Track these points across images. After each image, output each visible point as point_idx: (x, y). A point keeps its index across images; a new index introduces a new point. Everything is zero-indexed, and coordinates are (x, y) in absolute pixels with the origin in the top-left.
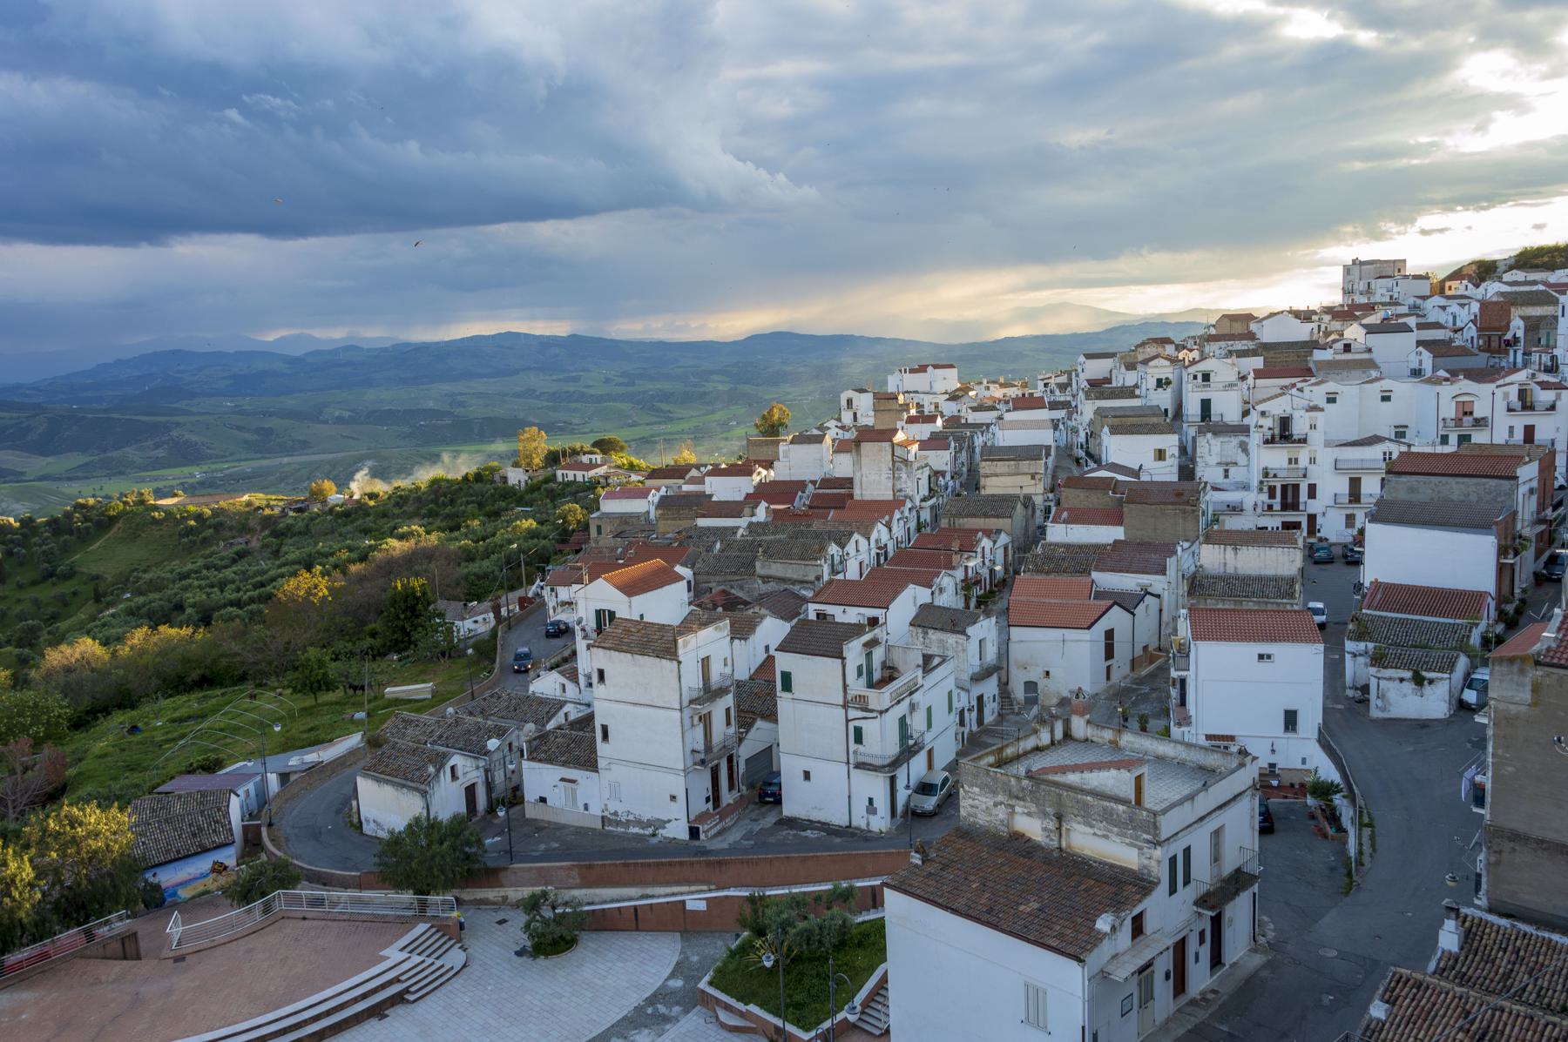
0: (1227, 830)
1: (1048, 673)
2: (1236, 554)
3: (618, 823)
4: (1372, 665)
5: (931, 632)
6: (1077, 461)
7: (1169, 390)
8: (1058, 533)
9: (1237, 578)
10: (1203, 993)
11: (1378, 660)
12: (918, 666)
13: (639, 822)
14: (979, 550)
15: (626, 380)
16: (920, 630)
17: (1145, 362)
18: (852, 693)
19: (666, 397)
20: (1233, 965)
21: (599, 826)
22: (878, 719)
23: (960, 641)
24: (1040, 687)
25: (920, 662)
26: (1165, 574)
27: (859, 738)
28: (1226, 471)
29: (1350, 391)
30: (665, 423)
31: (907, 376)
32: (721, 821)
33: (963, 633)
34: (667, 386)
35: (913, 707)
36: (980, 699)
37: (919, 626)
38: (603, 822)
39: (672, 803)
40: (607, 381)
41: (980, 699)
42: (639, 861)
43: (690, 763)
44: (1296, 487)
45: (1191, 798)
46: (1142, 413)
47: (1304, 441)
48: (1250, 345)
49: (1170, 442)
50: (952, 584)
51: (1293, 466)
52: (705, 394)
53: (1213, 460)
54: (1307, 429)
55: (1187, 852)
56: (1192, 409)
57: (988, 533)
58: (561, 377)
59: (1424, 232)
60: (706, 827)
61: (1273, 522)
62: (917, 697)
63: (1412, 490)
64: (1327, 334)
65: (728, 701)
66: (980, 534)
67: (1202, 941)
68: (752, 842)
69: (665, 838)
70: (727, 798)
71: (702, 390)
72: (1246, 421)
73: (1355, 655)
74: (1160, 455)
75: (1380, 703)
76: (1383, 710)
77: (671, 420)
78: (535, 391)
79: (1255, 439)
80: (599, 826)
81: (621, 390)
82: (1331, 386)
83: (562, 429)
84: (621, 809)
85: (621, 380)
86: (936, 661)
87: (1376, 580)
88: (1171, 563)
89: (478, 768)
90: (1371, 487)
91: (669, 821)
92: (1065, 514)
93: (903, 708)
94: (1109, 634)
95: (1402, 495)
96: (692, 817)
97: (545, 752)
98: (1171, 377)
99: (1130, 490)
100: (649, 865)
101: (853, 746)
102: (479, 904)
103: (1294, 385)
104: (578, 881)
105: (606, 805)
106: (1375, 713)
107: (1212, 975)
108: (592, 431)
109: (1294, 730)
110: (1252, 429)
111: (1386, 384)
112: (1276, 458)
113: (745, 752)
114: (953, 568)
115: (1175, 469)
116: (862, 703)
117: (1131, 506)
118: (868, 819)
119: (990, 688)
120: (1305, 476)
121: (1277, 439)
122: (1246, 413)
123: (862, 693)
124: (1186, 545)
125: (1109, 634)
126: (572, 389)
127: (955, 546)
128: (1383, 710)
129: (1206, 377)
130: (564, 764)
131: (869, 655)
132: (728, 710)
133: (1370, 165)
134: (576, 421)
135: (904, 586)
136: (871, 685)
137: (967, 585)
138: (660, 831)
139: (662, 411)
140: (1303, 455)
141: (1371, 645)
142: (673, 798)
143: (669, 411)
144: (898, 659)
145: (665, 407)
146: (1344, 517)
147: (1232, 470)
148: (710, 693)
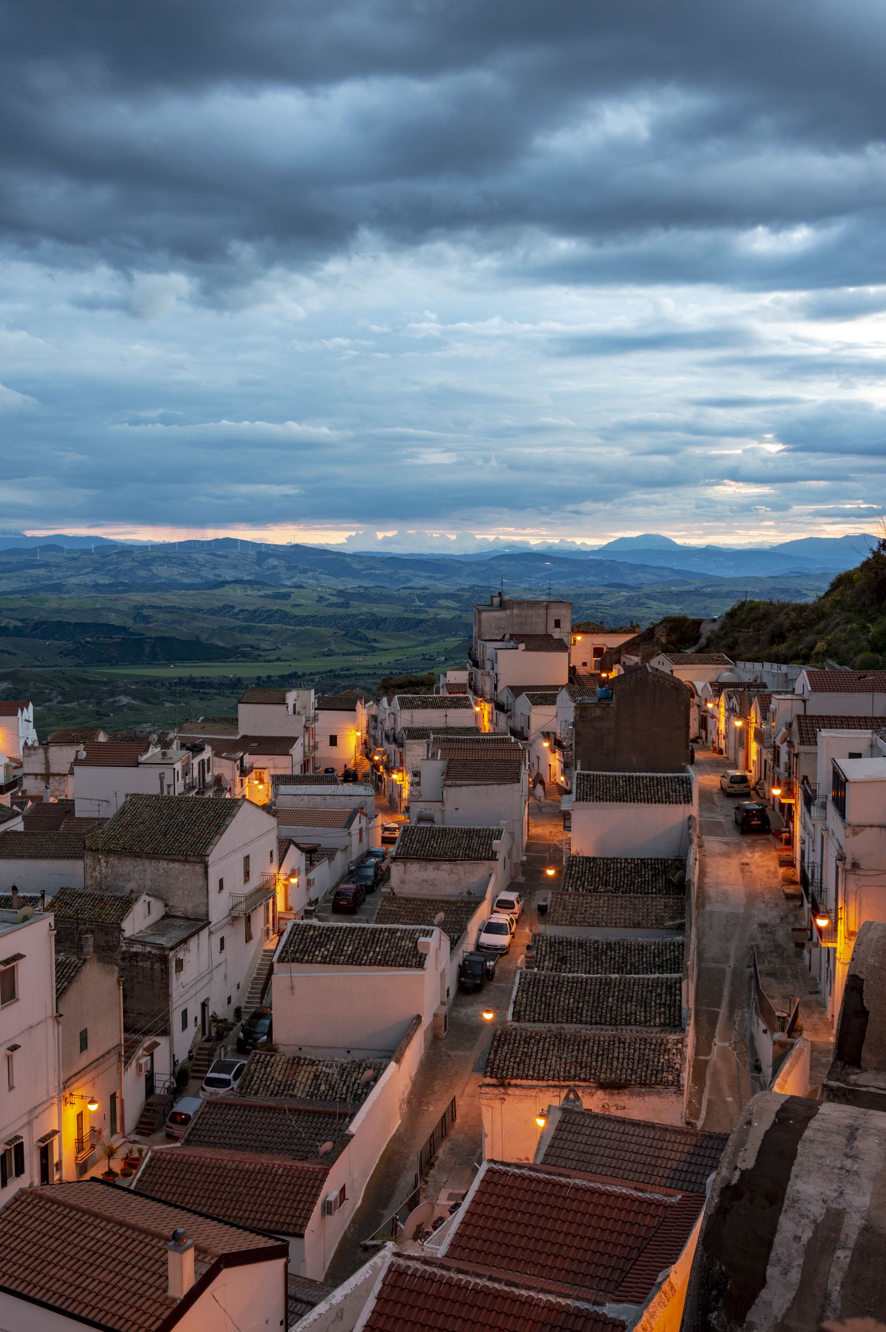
19: (376, 622)
34: (381, 610)
52: (421, 621)
58: (270, 592)
77: (374, 650)
78: (233, 607)
83: (245, 655)
108: (278, 659)
126: (275, 608)
134: (263, 646)
139: (366, 639)
143: (375, 640)
145: (371, 634)
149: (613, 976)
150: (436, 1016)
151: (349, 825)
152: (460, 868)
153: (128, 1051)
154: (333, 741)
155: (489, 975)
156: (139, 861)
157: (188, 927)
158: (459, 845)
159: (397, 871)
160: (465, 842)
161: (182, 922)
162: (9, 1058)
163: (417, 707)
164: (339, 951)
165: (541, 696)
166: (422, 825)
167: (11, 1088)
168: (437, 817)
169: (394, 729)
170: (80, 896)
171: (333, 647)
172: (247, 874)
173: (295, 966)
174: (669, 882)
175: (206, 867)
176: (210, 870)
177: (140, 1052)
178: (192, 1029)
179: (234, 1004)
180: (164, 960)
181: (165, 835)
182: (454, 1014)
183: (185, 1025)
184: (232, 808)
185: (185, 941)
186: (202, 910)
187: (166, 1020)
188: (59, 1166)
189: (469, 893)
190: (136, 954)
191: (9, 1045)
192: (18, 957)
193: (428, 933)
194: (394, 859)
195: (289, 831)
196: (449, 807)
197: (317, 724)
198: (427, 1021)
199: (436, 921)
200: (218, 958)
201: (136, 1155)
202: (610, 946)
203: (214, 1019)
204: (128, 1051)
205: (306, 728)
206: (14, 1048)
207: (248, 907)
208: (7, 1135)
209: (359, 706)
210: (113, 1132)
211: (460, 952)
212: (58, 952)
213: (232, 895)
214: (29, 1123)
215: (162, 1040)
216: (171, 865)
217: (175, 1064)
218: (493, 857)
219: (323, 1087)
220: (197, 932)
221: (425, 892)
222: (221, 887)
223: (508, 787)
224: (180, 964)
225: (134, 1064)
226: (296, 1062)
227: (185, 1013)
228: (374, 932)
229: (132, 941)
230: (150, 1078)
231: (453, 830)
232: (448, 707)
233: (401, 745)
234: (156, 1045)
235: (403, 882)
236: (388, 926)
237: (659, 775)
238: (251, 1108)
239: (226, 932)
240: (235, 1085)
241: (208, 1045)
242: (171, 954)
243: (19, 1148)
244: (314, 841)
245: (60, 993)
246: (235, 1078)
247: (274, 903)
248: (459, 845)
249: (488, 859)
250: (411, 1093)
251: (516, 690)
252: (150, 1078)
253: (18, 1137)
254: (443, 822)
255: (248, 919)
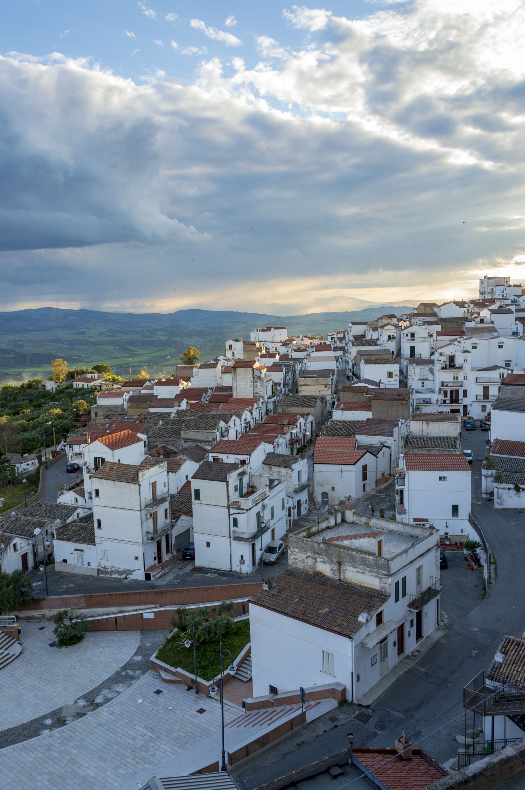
0: (424, 566)
1: (333, 488)
2: (428, 426)
3: (106, 573)
4: (495, 482)
5: (273, 467)
6: (348, 378)
7: (394, 341)
8: (338, 415)
9: (428, 438)
10: (412, 652)
11: (498, 479)
12: (267, 485)
13: (118, 572)
14: (298, 424)
15: (111, 334)
16: (267, 466)
17: (382, 327)
18: (232, 500)
19: (133, 343)
20: (428, 637)
21: (96, 574)
22: (245, 514)
23: (289, 472)
24: (329, 495)
25: (268, 483)
26: (392, 436)
27: (235, 524)
28: (423, 383)
29: (483, 342)
30: (132, 357)
31: (261, 333)
32: (162, 569)
33: (290, 467)
34: (133, 337)
35: (264, 507)
36: (299, 502)
37: (267, 464)
38: (98, 572)
39: (136, 561)
40: (101, 334)
41: (299, 502)
42: (118, 593)
43: (145, 539)
44: (457, 391)
45: (406, 551)
46: (380, 353)
47: (461, 368)
48: (434, 319)
49: (395, 368)
50: (284, 442)
51: (456, 381)
52: (153, 341)
53: (416, 377)
54: (462, 362)
55: (404, 579)
56: (406, 351)
57: (303, 415)
58: (76, 332)
59: (517, 263)
60: (154, 573)
61: (446, 409)
62: (266, 502)
63: (513, 393)
64: (472, 314)
65: (166, 505)
66: (298, 416)
67: (412, 625)
68: (179, 581)
69: (132, 580)
70: (166, 557)
71: (152, 339)
72: (433, 357)
73: (486, 477)
74: (390, 375)
75: (499, 501)
76: (501, 504)
77: (136, 355)
78: (61, 339)
79: (437, 367)
80: (96, 574)
81: (109, 339)
82: (474, 340)
84: (108, 564)
85: (108, 334)
86: (276, 482)
87: (497, 438)
88: (396, 430)
89: (28, 544)
90: (494, 391)
91: (134, 571)
92: (342, 405)
93: (258, 508)
94: (365, 467)
95: (508, 396)
96: (147, 568)
97: (66, 535)
98: (395, 335)
99: (375, 393)
100: (123, 595)
101: (232, 528)
102: (29, 619)
103: (456, 340)
104: (84, 604)
105: (100, 563)
106: (497, 506)
107: (417, 643)
108: (92, 361)
109: (457, 515)
110: (436, 362)
111: (501, 340)
112: (447, 377)
113: (175, 532)
114: (285, 434)
115: (397, 382)
116: (237, 506)
117: (376, 401)
118: (240, 567)
119: (304, 496)
120: (461, 386)
121: (448, 367)
122: (432, 354)
123: (237, 500)
124: (403, 421)
125: (365, 467)
126: (82, 339)
127: (286, 422)
128: (501, 504)
129: (413, 335)
130: (77, 541)
131: (241, 480)
132: (166, 510)
133: (490, 229)
134: (83, 355)
135: (259, 444)
136: (242, 496)
137: (292, 442)
138: (130, 576)
139: (130, 350)
140: (461, 375)
141: (494, 472)
142: (136, 558)
143: (134, 351)
144: (256, 482)
145: (132, 348)
146: (481, 407)
147: (426, 383)
148: (156, 501)
171: (116, 354)
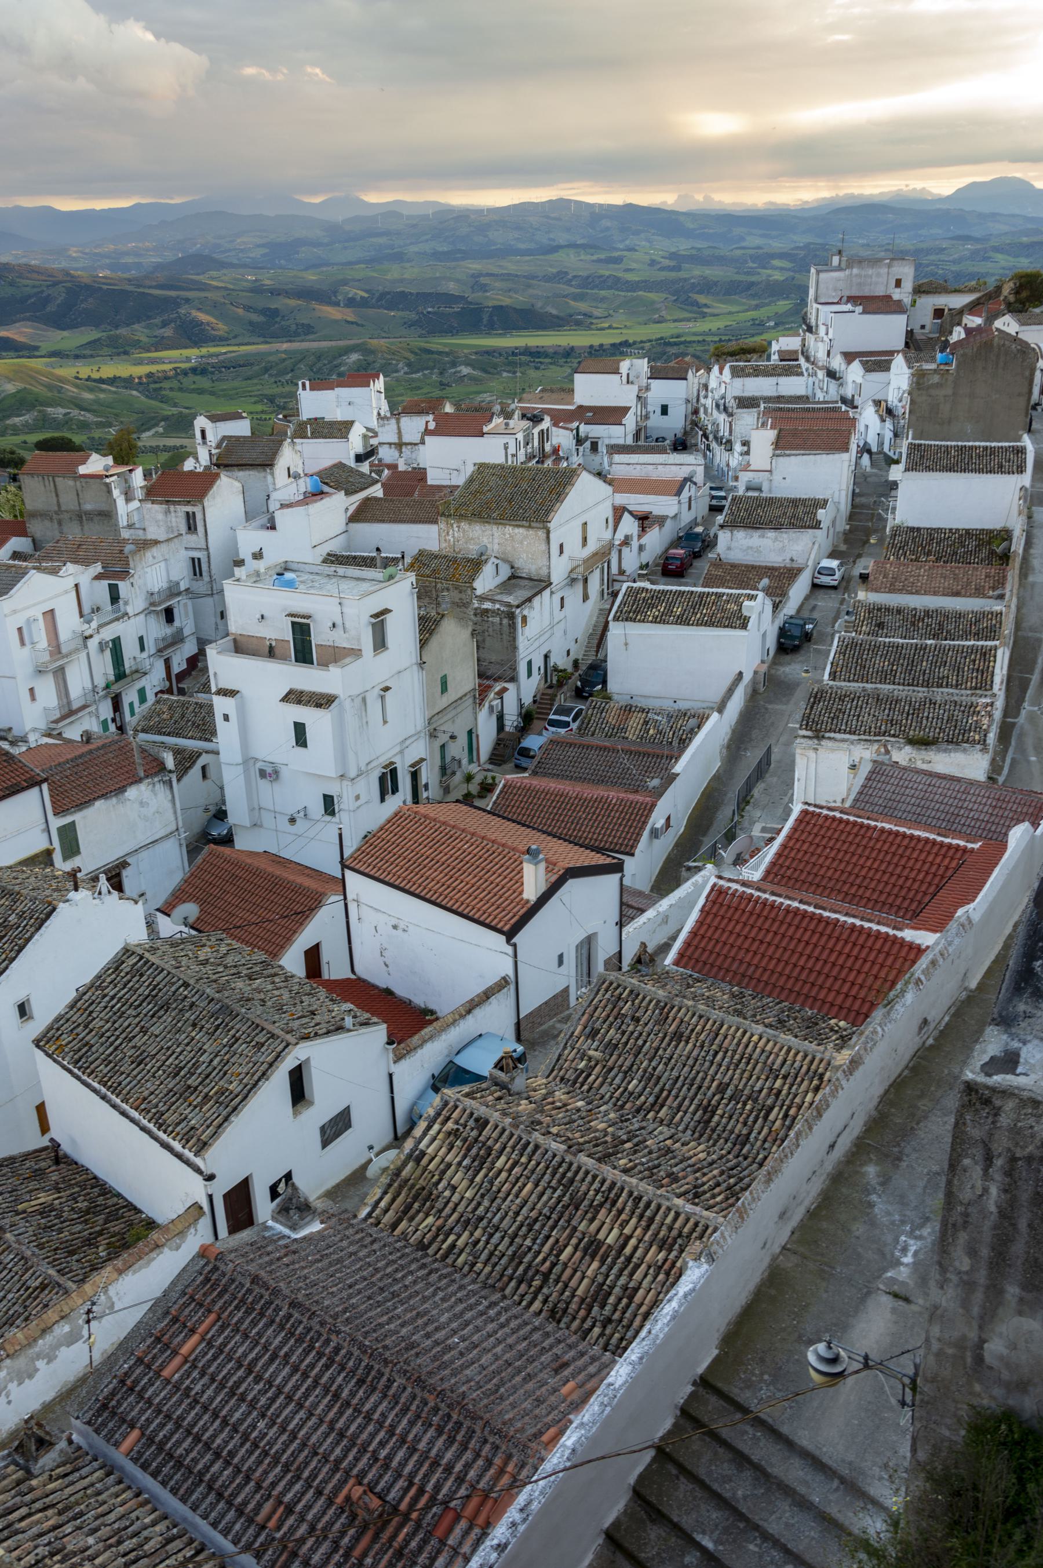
15: (672, 263)
30: (695, 319)
77: (704, 315)
85: (667, 262)
149: (929, 642)
150: (756, 673)
151: (678, 493)
152: (785, 536)
153: (481, 694)
154: (664, 410)
155: (807, 637)
156: (488, 526)
157: (532, 588)
158: (785, 514)
159: (724, 538)
160: (790, 512)
161: (526, 582)
162: (382, 697)
163: (748, 375)
164: (669, 612)
165: (875, 363)
166: (750, 494)
167: (385, 722)
168: (765, 487)
169: (723, 397)
170: (436, 557)
171: (663, 313)
172: (585, 540)
173: (629, 624)
174: (992, 553)
175: (548, 532)
176: (552, 535)
177: (492, 695)
178: (536, 678)
179: (573, 656)
180: (511, 616)
181: (510, 502)
182: (773, 672)
183: (530, 674)
184: (571, 477)
185: (529, 600)
186: (544, 572)
187: (514, 669)
188: (426, 786)
189: (792, 560)
190: (487, 611)
191: (382, 686)
192: (386, 611)
193: (752, 598)
194: (722, 527)
195: (621, 499)
196: (777, 477)
197: (650, 394)
198: (747, 677)
199: (760, 586)
200: (558, 615)
201: (490, 781)
202: (927, 613)
203: (555, 669)
204: (481, 694)
205: (639, 398)
206: (386, 689)
207: (585, 570)
208: (384, 760)
209: (690, 374)
210: (471, 761)
211: (781, 615)
212: (420, 607)
213: (571, 559)
214: (401, 752)
215: (510, 686)
216: (517, 530)
217: (521, 706)
218: (817, 526)
219: (651, 732)
220: (540, 592)
221: (750, 559)
222: (561, 552)
223: (837, 456)
224: (524, 619)
225: (487, 705)
226: (628, 709)
227: (530, 663)
228: (702, 595)
229: (482, 598)
230: (500, 718)
231: (780, 500)
232: (779, 375)
233: (731, 415)
234: (505, 690)
235: (729, 549)
236: (715, 590)
237: (993, 444)
238: (589, 747)
239: (567, 593)
240: (574, 726)
241: (550, 691)
242: (518, 611)
243: (394, 772)
244: (646, 508)
245: (423, 643)
246: (574, 720)
247: (609, 567)
248: (785, 514)
249: (812, 528)
250: (730, 740)
251: (849, 357)
252: (500, 718)
253: (392, 763)
254: (770, 491)
255: (586, 581)
